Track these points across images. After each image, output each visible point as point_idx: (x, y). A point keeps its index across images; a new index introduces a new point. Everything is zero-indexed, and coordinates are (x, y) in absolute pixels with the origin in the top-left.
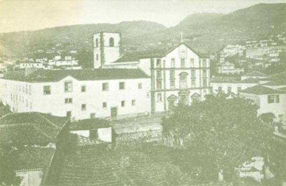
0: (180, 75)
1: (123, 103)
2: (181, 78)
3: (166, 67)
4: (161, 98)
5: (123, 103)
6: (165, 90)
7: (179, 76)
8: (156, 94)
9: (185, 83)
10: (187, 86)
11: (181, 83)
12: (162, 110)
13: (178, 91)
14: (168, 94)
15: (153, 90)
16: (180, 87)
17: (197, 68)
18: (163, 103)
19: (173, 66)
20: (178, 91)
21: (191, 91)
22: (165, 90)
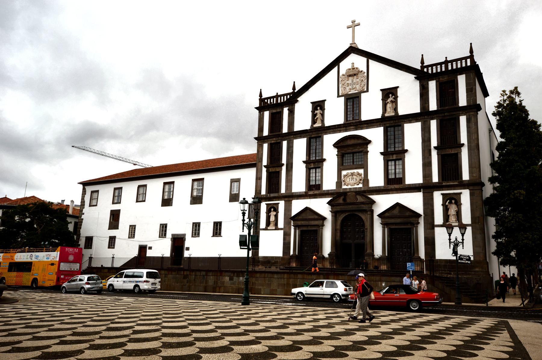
0: (336, 145)
1: (196, 227)
2: (341, 157)
3: (297, 127)
4: (276, 216)
5: (196, 227)
6: (290, 197)
7: (335, 151)
8: (263, 206)
9: (361, 171)
10: (366, 181)
11: (344, 173)
12: (278, 252)
13: (328, 199)
14: (297, 206)
15: (259, 196)
16: (339, 183)
17: (411, 118)
18: (281, 232)
19: (317, 125)
20: (328, 199)
21: (374, 197)
22: (290, 197)
